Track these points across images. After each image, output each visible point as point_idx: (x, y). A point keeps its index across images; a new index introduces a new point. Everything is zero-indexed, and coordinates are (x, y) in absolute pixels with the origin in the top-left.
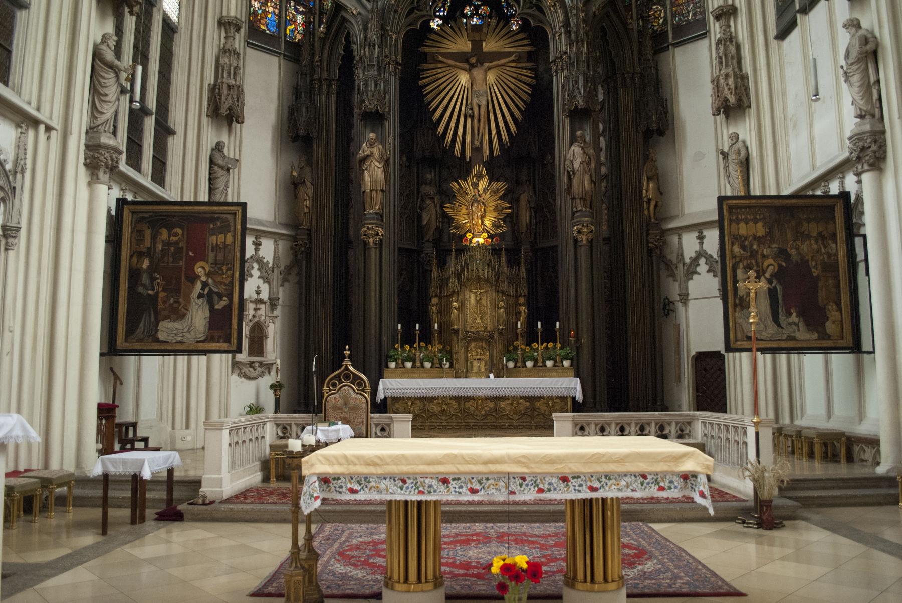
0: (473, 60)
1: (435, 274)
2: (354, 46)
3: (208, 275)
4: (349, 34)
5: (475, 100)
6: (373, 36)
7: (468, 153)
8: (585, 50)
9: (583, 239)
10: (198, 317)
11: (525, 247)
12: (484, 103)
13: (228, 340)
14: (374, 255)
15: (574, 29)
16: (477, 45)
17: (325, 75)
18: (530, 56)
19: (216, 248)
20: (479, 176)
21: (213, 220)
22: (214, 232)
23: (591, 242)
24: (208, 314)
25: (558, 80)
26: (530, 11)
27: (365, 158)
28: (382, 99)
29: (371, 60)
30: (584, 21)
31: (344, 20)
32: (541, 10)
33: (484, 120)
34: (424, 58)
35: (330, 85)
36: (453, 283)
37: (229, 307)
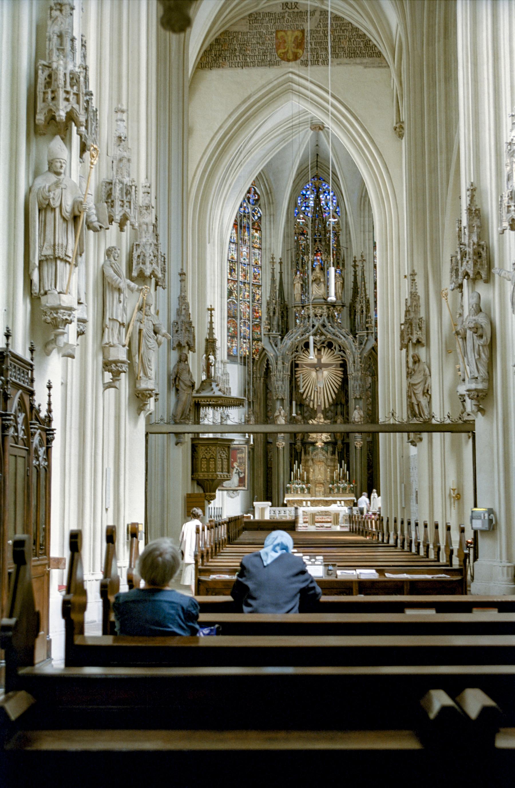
0: (318, 369)
1: (303, 457)
2: (271, 366)
3: (238, 466)
4: (268, 360)
5: (319, 386)
6: (280, 366)
7: (315, 406)
8: (360, 374)
9: (358, 446)
10: (235, 479)
11: (339, 443)
12: (322, 387)
13: (244, 486)
14: (281, 452)
15: (356, 365)
16: (319, 360)
17: (258, 375)
18: (342, 365)
19: (240, 458)
20: (320, 418)
21: (239, 449)
22: (239, 453)
23: (361, 448)
24: (238, 478)
25: (351, 383)
26: (340, 353)
27: (277, 416)
28: (284, 394)
29: (280, 377)
30: (361, 362)
31: (266, 354)
32: (344, 352)
33: (322, 393)
34: (297, 365)
35: (260, 379)
36: (310, 463)
37: (244, 477)
